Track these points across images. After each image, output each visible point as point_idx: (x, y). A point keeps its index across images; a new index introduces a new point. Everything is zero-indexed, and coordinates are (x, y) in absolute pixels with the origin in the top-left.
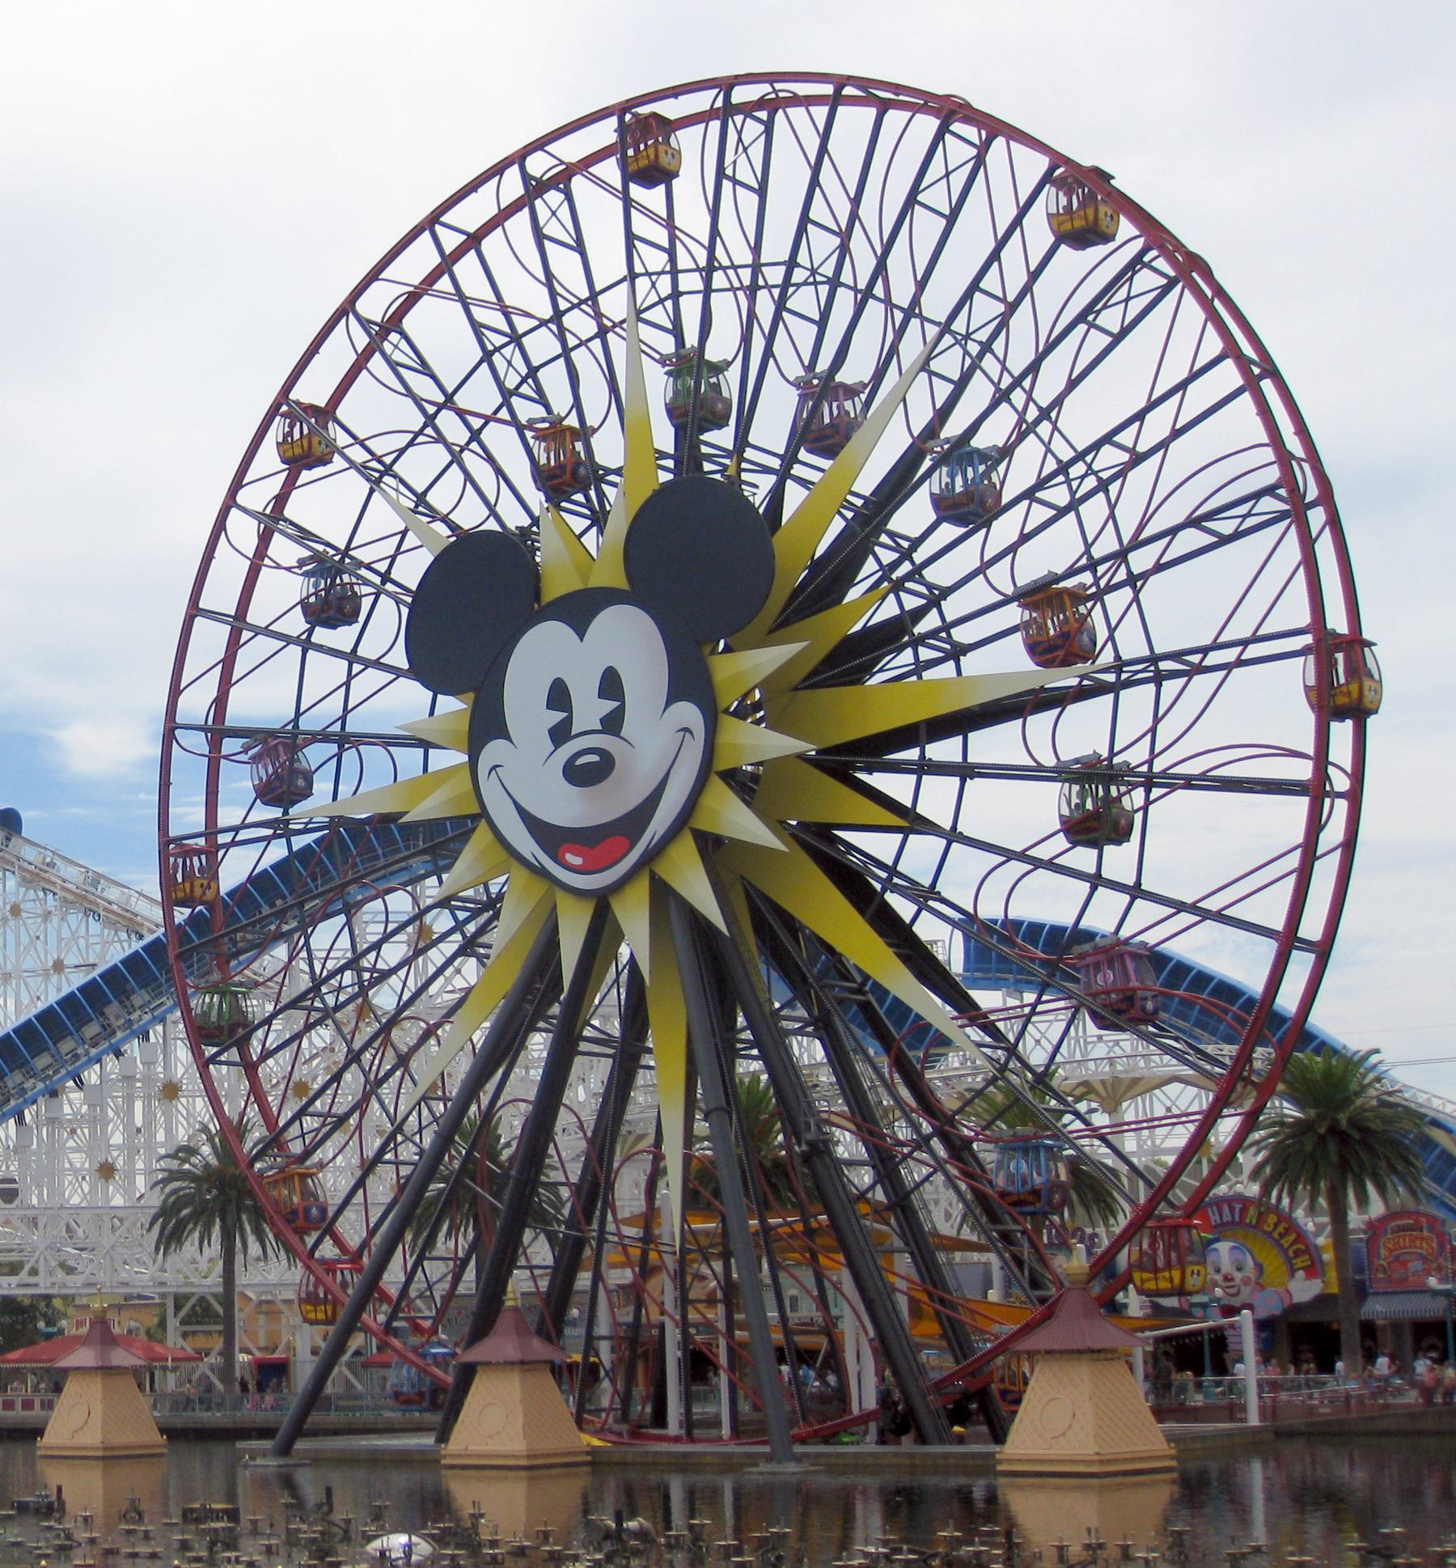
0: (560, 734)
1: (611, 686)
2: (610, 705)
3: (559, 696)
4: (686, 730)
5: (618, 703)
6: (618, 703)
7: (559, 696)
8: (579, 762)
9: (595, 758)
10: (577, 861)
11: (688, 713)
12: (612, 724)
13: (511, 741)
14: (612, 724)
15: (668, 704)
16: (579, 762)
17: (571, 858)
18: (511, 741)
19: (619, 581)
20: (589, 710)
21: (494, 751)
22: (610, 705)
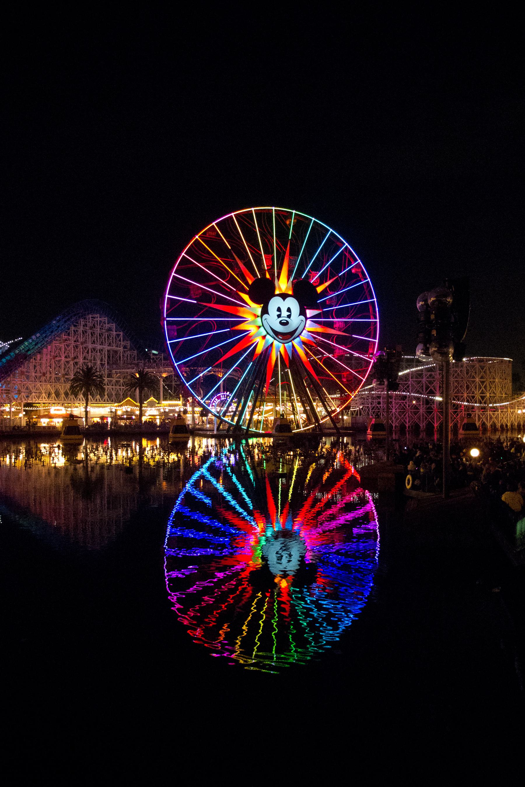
0: (279, 316)
1: (289, 310)
2: (290, 313)
6: (290, 313)
7: (279, 310)
9: (285, 321)
10: (281, 338)
11: (302, 317)
13: (269, 314)
14: (289, 316)
15: (299, 315)
16: (282, 321)
17: (279, 337)
18: (269, 314)
19: (290, 293)
20: (285, 313)
21: (265, 316)
22: (289, 313)
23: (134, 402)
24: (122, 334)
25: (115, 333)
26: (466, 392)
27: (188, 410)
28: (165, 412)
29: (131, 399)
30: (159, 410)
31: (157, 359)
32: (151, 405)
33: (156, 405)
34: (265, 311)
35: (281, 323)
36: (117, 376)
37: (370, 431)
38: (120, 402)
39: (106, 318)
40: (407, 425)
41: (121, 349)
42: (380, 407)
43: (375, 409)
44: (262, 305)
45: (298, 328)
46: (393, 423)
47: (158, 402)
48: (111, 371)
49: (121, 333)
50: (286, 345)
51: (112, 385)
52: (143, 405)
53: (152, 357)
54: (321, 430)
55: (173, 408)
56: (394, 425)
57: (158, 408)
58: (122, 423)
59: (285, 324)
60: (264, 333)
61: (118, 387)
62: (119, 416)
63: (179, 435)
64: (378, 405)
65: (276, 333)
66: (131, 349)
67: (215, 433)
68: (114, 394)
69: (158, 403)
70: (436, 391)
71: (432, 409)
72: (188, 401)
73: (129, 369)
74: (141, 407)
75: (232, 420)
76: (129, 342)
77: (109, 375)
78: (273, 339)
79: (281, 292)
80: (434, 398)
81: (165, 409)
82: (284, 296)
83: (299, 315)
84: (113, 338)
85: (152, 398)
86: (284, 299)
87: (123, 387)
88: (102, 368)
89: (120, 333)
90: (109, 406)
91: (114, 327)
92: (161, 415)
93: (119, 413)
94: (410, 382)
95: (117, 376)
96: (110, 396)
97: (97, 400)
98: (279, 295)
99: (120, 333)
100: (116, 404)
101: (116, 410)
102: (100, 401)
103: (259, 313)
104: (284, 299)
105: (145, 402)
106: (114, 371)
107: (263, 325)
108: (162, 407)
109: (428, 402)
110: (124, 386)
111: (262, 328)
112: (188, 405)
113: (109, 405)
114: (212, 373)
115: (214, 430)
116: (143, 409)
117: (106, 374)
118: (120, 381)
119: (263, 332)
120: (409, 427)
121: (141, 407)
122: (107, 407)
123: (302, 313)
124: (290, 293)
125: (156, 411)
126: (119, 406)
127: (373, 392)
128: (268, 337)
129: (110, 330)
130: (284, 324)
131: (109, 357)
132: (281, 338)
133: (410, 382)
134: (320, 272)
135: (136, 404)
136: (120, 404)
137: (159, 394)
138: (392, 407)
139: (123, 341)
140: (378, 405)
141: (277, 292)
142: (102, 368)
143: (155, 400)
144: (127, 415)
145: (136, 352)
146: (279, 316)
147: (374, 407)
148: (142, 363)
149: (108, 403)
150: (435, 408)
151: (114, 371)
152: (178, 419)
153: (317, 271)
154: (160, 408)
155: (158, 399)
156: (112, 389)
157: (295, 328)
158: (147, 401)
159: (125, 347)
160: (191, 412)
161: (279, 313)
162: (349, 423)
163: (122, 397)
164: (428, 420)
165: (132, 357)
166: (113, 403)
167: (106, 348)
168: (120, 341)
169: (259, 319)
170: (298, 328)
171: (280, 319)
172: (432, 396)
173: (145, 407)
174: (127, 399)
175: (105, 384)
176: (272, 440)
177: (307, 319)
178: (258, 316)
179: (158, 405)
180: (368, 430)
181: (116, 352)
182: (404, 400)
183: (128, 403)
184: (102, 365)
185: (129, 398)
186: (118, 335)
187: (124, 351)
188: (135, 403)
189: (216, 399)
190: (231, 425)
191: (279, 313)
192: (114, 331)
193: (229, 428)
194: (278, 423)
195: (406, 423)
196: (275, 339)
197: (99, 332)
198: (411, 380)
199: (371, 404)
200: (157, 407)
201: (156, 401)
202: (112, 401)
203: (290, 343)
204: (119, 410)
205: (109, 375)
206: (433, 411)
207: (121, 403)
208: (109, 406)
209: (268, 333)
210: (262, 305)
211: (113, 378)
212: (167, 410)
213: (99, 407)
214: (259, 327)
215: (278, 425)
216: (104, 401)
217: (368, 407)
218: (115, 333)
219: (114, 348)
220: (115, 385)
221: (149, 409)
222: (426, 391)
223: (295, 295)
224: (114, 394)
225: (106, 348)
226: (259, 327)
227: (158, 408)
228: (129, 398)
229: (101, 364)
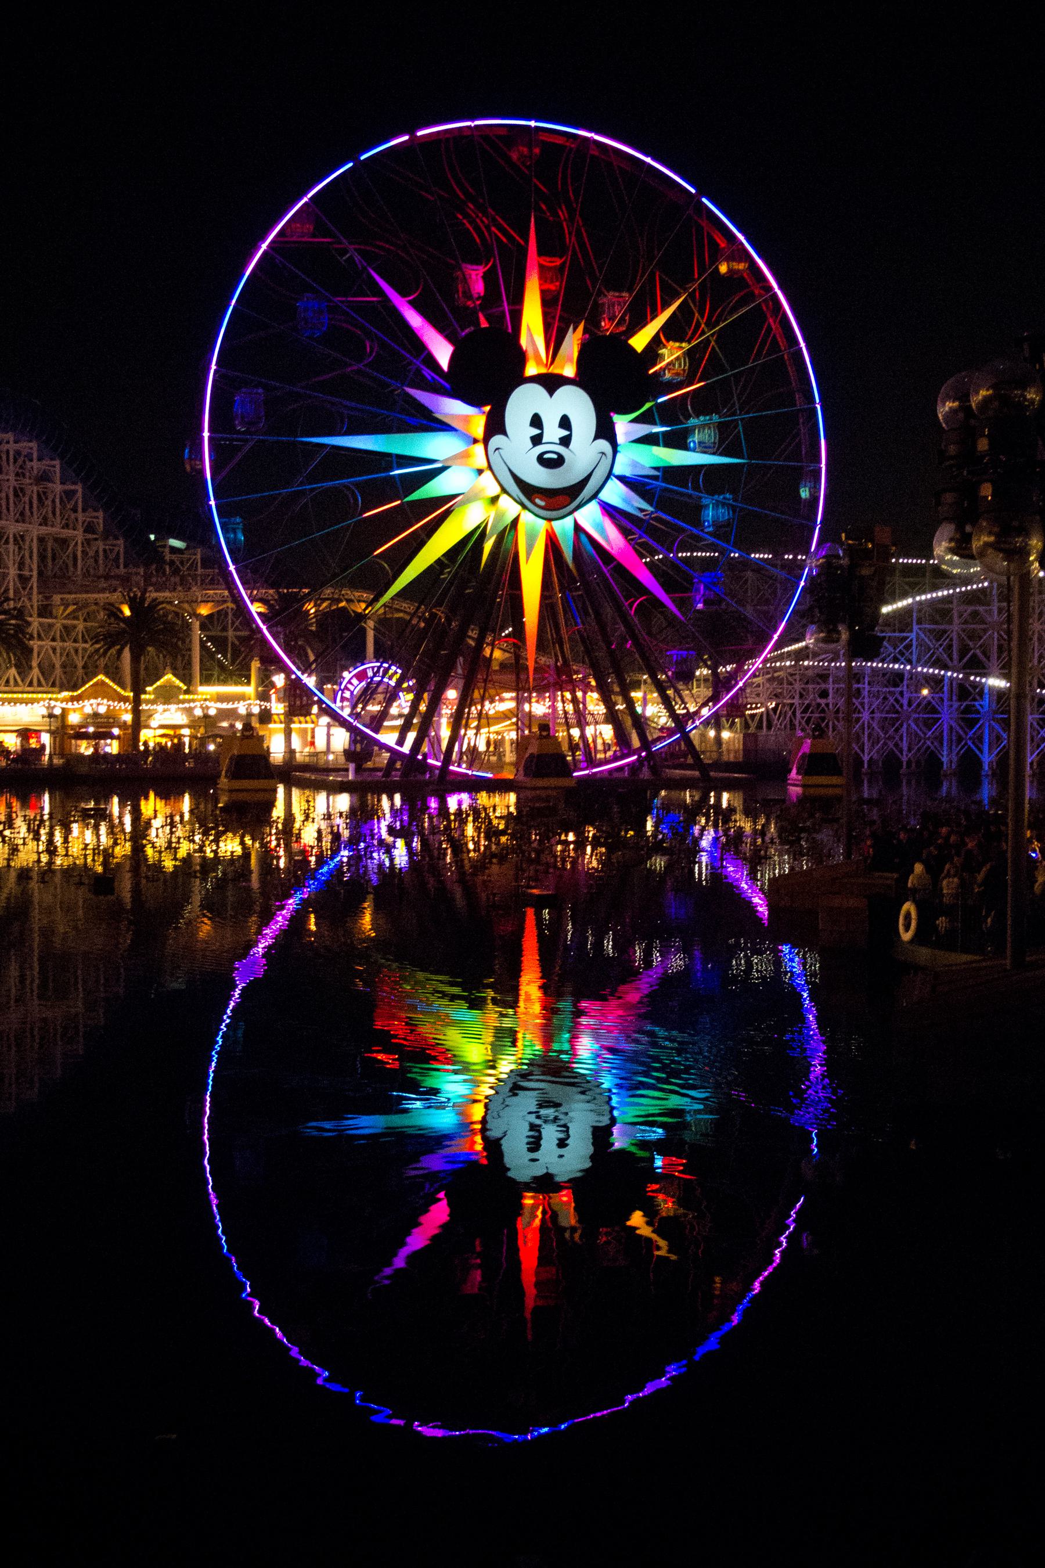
0: (537, 440)
1: (565, 423)
2: (565, 433)
3: (536, 421)
4: (603, 453)
7: (536, 421)
9: (555, 456)
10: (542, 504)
11: (604, 445)
14: (565, 441)
16: (546, 456)
17: (538, 501)
20: (553, 432)
21: (497, 440)
22: (565, 433)
23: (116, 687)
24: (80, 490)
25: (58, 488)
27: (273, 711)
28: (206, 716)
29: (107, 680)
30: (189, 711)
31: (182, 563)
32: (167, 696)
33: (182, 697)
34: (496, 426)
35: (542, 460)
36: (68, 612)
37: (798, 773)
38: (75, 688)
39: (34, 445)
40: (904, 759)
41: (79, 535)
42: (827, 705)
43: (812, 712)
44: (487, 408)
46: (863, 751)
47: (185, 688)
48: (47, 598)
49: (79, 488)
50: (556, 524)
51: (54, 640)
52: (143, 697)
53: (168, 557)
54: (654, 770)
55: (230, 706)
56: (866, 758)
57: (187, 705)
58: (85, 749)
59: (553, 463)
60: (495, 490)
61: (69, 645)
62: (72, 727)
63: (246, 784)
64: (819, 700)
65: (529, 491)
66: (106, 535)
67: (350, 778)
68: (58, 665)
69: (187, 692)
70: (988, 658)
72: (273, 685)
73: (103, 590)
74: (137, 702)
75: (401, 742)
76: (101, 514)
77: (45, 611)
78: (519, 507)
79: (543, 370)
80: (984, 680)
81: (208, 708)
82: (551, 383)
83: (596, 437)
84: (53, 501)
85: (169, 677)
87: (87, 646)
88: (24, 589)
89: (73, 487)
90: (44, 700)
91: (58, 469)
92: (193, 725)
93: (74, 719)
94: (913, 635)
95: (68, 612)
96: (46, 671)
97: (8, 681)
98: (537, 379)
99: (73, 487)
100: (66, 694)
101: (63, 709)
102: (16, 684)
103: (478, 431)
105: (149, 689)
106: (57, 598)
107: (490, 467)
108: (198, 704)
109: (967, 692)
110: (86, 642)
111: (487, 474)
112: (273, 697)
113: (44, 696)
114: (343, 604)
115: (347, 770)
116: (144, 707)
117: (35, 607)
118: (75, 627)
119: (489, 485)
120: (909, 762)
121: (137, 702)
122: (38, 701)
123: (605, 431)
125: (179, 713)
126: (73, 699)
127: (806, 663)
128: (505, 501)
129: (44, 477)
130: (553, 463)
131: (42, 558)
132: (542, 504)
133: (913, 635)
135: (122, 692)
136: (75, 694)
137: (189, 664)
138: (862, 704)
139: (84, 510)
140: (819, 700)
141: (532, 369)
142: (24, 589)
143: (177, 682)
144: (97, 725)
145: (121, 542)
146: (537, 440)
147: (809, 706)
148: (137, 574)
149: (40, 689)
151: (57, 598)
152: (244, 737)
154: (192, 705)
155: (187, 679)
156: (54, 649)
157: (586, 475)
158: (155, 686)
159: (89, 529)
160: (282, 717)
161: (538, 432)
162: (736, 752)
163: (80, 671)
164: (966, 744)
165: (112, 556)
166: (56, 689)
167: (35, 531)
168: (75, 510)
171: (540, 449)
172: (976, 675)
173: (148, 702)
174: (95, 680)
175: (32, 638)
176: (512, 797)
178: (475, 441)
179: (187, 697)
180: (790, 771)
181: (64, 542)
182: (896, 685)
183: (100, 691)
184: (24, 580)
185: (101, 677)
186: (69, 494)
187: (88, 542)
188: (119, 689)
189: (355, 681)
190: (395, 754)
191: (538, 432)
192: (58, 482)
193: (392, 762)
194: (533, 749)
195: (901, 751)
196: (524, 507)
197: (13, 483)
198: (915, 627)
199: (801, 696)
200: (183, 702)
201: (181, 685)
202: (53, 685)
204: (74, 710)
205: (45, 611)
206: (978, 719)
207: (79, 692)
208: (44, 700)
209: (504, 490)
210: (487, 408)
211: (56, 618)
212: (212, 712)
213: (16, 701)
214: (480, 472)
215: (532, 755)
216: (31, 684)
217: (792, 705)
218: (58, 488)
219: (56, 530)
220: (63, 640)
221: (160, 708)
222: (960, 661)
224: (58, 665)
225: (35, 531)
226: (480, 472)
227: (187, 705)
228: (101, 677)
229: (20, 576)
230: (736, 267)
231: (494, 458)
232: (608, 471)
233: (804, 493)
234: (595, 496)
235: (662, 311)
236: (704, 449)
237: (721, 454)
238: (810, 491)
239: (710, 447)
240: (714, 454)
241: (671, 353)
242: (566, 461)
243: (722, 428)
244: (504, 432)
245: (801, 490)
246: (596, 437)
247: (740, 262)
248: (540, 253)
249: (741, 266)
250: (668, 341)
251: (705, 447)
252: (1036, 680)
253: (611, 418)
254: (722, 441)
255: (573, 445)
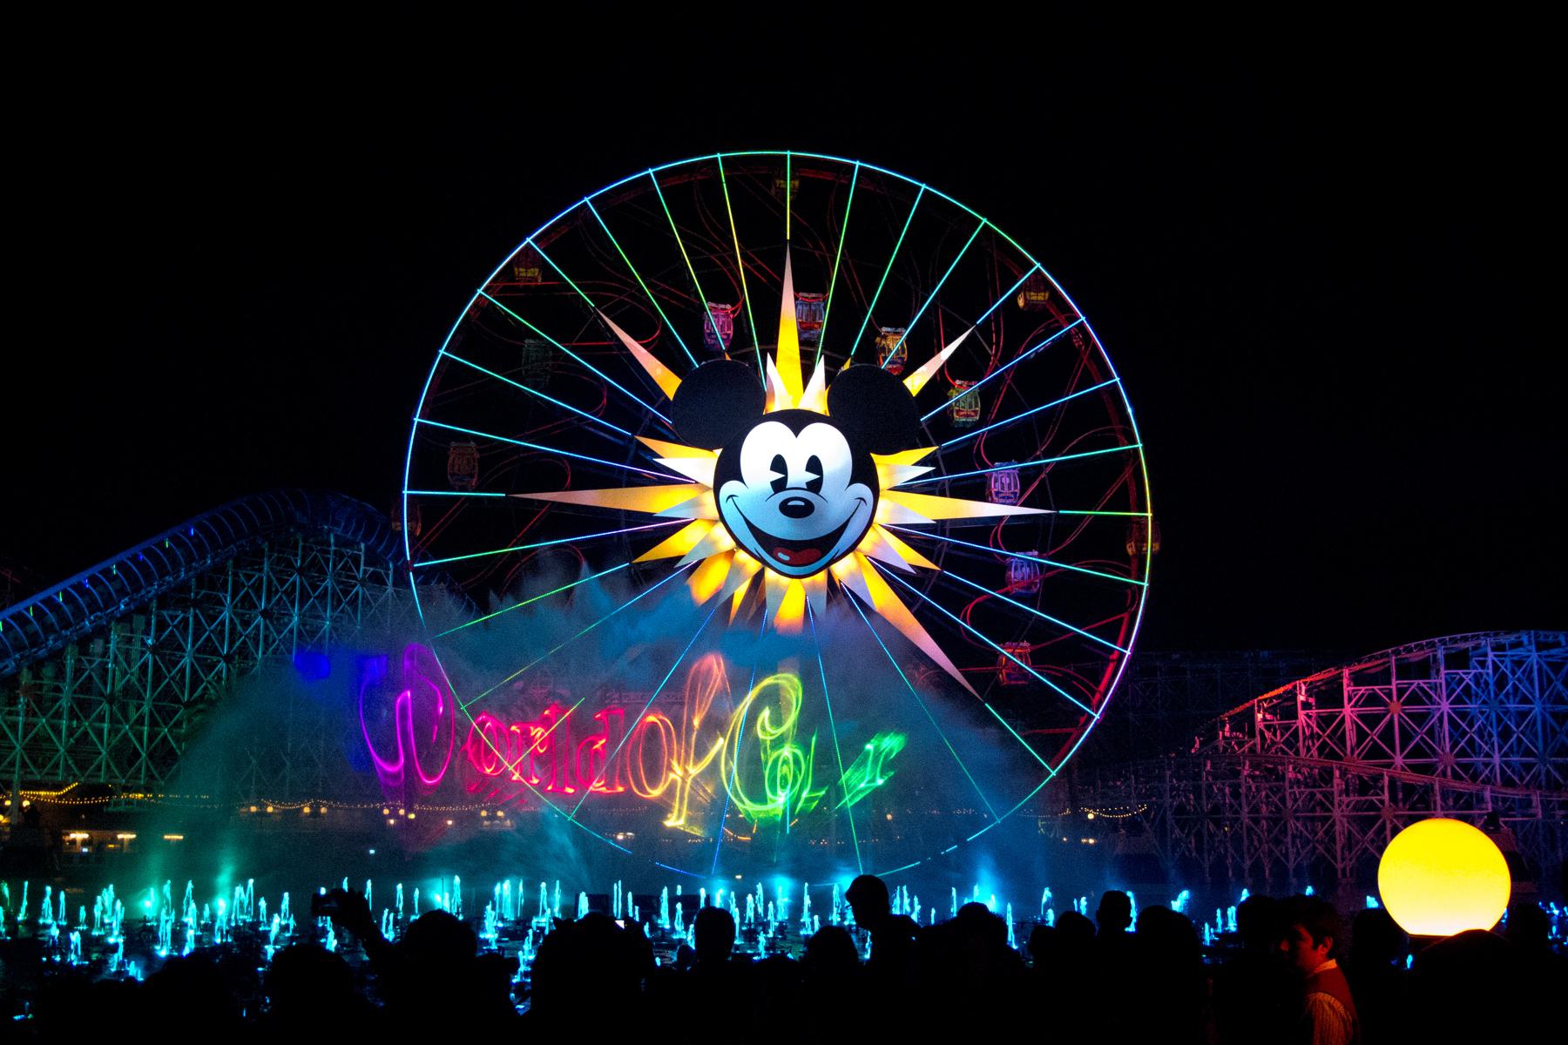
0: (779, 486)
1: (814, 465)
2: (813, 477)
3: (779, 464)
4: (862, 499)
5: (816, 477)
6: (816, 477)
7: (779, 464)
8: (790, 504)
9: (803, 504)
10: (786, 558)
11: (863, 490)
12: (815, 486)
14: (815, 486)
16: (790, 504)
17: (781, 555)
20: (798, 475)
21: (730, 487)
22: (813, 477)
26: (1500, 748)
34: (729, 470)
35: (785, 508)
44: (718, 452)
45: (848, 521)
60: (729, 543)
65: (768, 542)
71: (1378, 809)
82: (797, 420)
83: (853, 480)
86: (797, 436)
104: (797, 436)
107: (722, 518)
111: (721, 525)
123: (863, 473)
124: (821, 407)
128: (741, 556)
134: (906, 329)
141: (773, 407)
150: (1387, 802)
153: (897, 327)
161: (780, 476)
169: (709, 497)
170: (848, 521)
171: (783, 496)
177: (876, 492)
191: (780, 476)
203: (821, 577)
206: (1378, 817)
209: (740, 545)
210: (718, 452)
223: (837, 417)
230: (1034, 298)
231: (727, 508)
232: (866, 522)
233: (1130, 550)
234: (853, 548)
235: (946, 346)
236: (1006, 500)
237: (1024, 505)
238: (1136, 546)
239: (1009, 498)
240: (1015, 505)
241: (962, 395)
242: (816, 506)
243: (1026, 477)
244: (741, 480)
245: (1128, 546)
246: (853, 480)
247: (1038, 291)
248: (797, 289)
249: (1041, 297)
250: (954, 380)
251: (1003, 498)
252: (1449, 770)
253: (871, 459)
254: (1023, 491)
255: (824, 491)
